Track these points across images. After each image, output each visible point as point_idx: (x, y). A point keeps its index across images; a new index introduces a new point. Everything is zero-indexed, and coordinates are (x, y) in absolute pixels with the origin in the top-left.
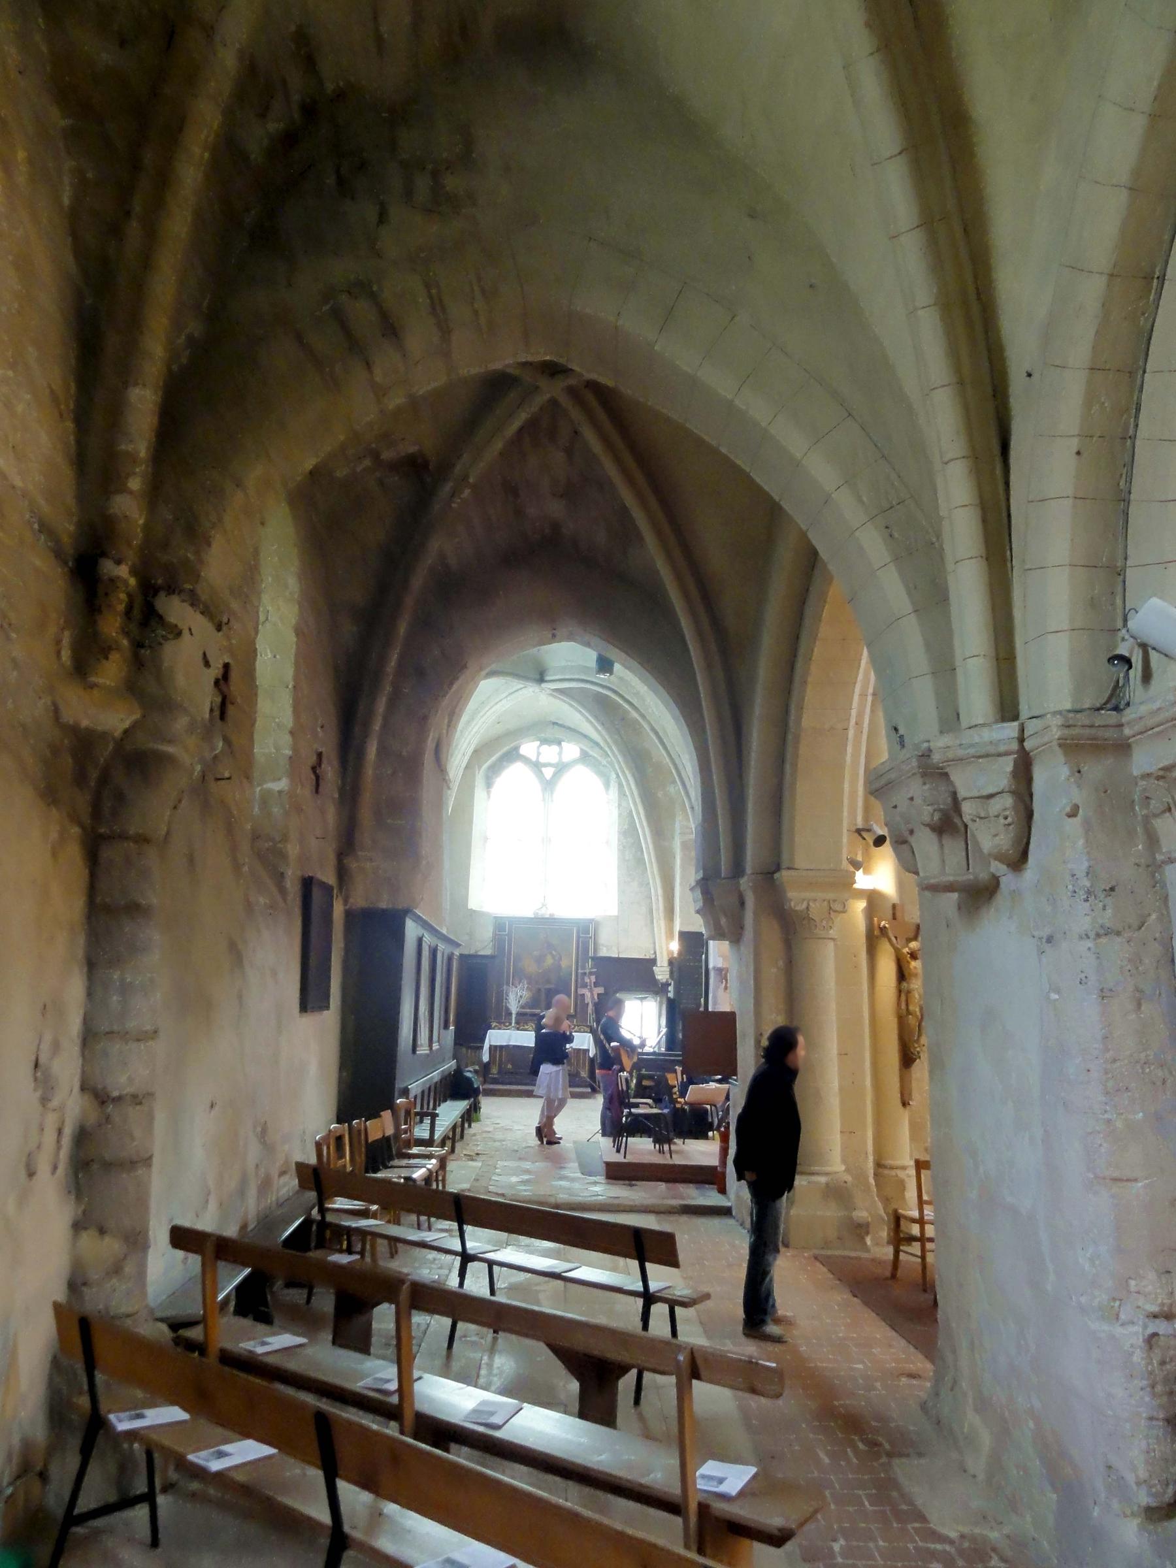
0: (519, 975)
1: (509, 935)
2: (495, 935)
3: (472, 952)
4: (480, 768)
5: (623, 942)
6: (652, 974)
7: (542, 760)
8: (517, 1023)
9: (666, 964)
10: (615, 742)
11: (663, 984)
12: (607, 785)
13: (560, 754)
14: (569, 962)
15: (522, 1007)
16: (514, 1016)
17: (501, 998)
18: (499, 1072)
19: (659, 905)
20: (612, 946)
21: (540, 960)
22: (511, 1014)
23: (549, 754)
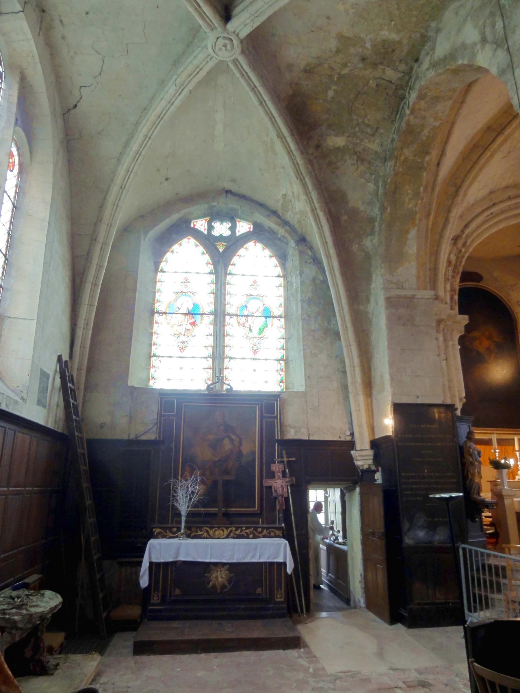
0: (190, 464)
2: (160, 415)
3: (132, 437)
4: (146, 233)
5: (314, 423)
6: (351, 458)
7: (216, 233)
8: (188, 528)
9: (368, 446)
11: (363, 471)
12: (282, 258)
13: (233, 229)
14: (251, 446)
15: (195, 506)
16: (183, 519)
17: (168, 494)
19: (354, 376)
21: (215, 445)
22: (179, 515)
23: (221, 229)
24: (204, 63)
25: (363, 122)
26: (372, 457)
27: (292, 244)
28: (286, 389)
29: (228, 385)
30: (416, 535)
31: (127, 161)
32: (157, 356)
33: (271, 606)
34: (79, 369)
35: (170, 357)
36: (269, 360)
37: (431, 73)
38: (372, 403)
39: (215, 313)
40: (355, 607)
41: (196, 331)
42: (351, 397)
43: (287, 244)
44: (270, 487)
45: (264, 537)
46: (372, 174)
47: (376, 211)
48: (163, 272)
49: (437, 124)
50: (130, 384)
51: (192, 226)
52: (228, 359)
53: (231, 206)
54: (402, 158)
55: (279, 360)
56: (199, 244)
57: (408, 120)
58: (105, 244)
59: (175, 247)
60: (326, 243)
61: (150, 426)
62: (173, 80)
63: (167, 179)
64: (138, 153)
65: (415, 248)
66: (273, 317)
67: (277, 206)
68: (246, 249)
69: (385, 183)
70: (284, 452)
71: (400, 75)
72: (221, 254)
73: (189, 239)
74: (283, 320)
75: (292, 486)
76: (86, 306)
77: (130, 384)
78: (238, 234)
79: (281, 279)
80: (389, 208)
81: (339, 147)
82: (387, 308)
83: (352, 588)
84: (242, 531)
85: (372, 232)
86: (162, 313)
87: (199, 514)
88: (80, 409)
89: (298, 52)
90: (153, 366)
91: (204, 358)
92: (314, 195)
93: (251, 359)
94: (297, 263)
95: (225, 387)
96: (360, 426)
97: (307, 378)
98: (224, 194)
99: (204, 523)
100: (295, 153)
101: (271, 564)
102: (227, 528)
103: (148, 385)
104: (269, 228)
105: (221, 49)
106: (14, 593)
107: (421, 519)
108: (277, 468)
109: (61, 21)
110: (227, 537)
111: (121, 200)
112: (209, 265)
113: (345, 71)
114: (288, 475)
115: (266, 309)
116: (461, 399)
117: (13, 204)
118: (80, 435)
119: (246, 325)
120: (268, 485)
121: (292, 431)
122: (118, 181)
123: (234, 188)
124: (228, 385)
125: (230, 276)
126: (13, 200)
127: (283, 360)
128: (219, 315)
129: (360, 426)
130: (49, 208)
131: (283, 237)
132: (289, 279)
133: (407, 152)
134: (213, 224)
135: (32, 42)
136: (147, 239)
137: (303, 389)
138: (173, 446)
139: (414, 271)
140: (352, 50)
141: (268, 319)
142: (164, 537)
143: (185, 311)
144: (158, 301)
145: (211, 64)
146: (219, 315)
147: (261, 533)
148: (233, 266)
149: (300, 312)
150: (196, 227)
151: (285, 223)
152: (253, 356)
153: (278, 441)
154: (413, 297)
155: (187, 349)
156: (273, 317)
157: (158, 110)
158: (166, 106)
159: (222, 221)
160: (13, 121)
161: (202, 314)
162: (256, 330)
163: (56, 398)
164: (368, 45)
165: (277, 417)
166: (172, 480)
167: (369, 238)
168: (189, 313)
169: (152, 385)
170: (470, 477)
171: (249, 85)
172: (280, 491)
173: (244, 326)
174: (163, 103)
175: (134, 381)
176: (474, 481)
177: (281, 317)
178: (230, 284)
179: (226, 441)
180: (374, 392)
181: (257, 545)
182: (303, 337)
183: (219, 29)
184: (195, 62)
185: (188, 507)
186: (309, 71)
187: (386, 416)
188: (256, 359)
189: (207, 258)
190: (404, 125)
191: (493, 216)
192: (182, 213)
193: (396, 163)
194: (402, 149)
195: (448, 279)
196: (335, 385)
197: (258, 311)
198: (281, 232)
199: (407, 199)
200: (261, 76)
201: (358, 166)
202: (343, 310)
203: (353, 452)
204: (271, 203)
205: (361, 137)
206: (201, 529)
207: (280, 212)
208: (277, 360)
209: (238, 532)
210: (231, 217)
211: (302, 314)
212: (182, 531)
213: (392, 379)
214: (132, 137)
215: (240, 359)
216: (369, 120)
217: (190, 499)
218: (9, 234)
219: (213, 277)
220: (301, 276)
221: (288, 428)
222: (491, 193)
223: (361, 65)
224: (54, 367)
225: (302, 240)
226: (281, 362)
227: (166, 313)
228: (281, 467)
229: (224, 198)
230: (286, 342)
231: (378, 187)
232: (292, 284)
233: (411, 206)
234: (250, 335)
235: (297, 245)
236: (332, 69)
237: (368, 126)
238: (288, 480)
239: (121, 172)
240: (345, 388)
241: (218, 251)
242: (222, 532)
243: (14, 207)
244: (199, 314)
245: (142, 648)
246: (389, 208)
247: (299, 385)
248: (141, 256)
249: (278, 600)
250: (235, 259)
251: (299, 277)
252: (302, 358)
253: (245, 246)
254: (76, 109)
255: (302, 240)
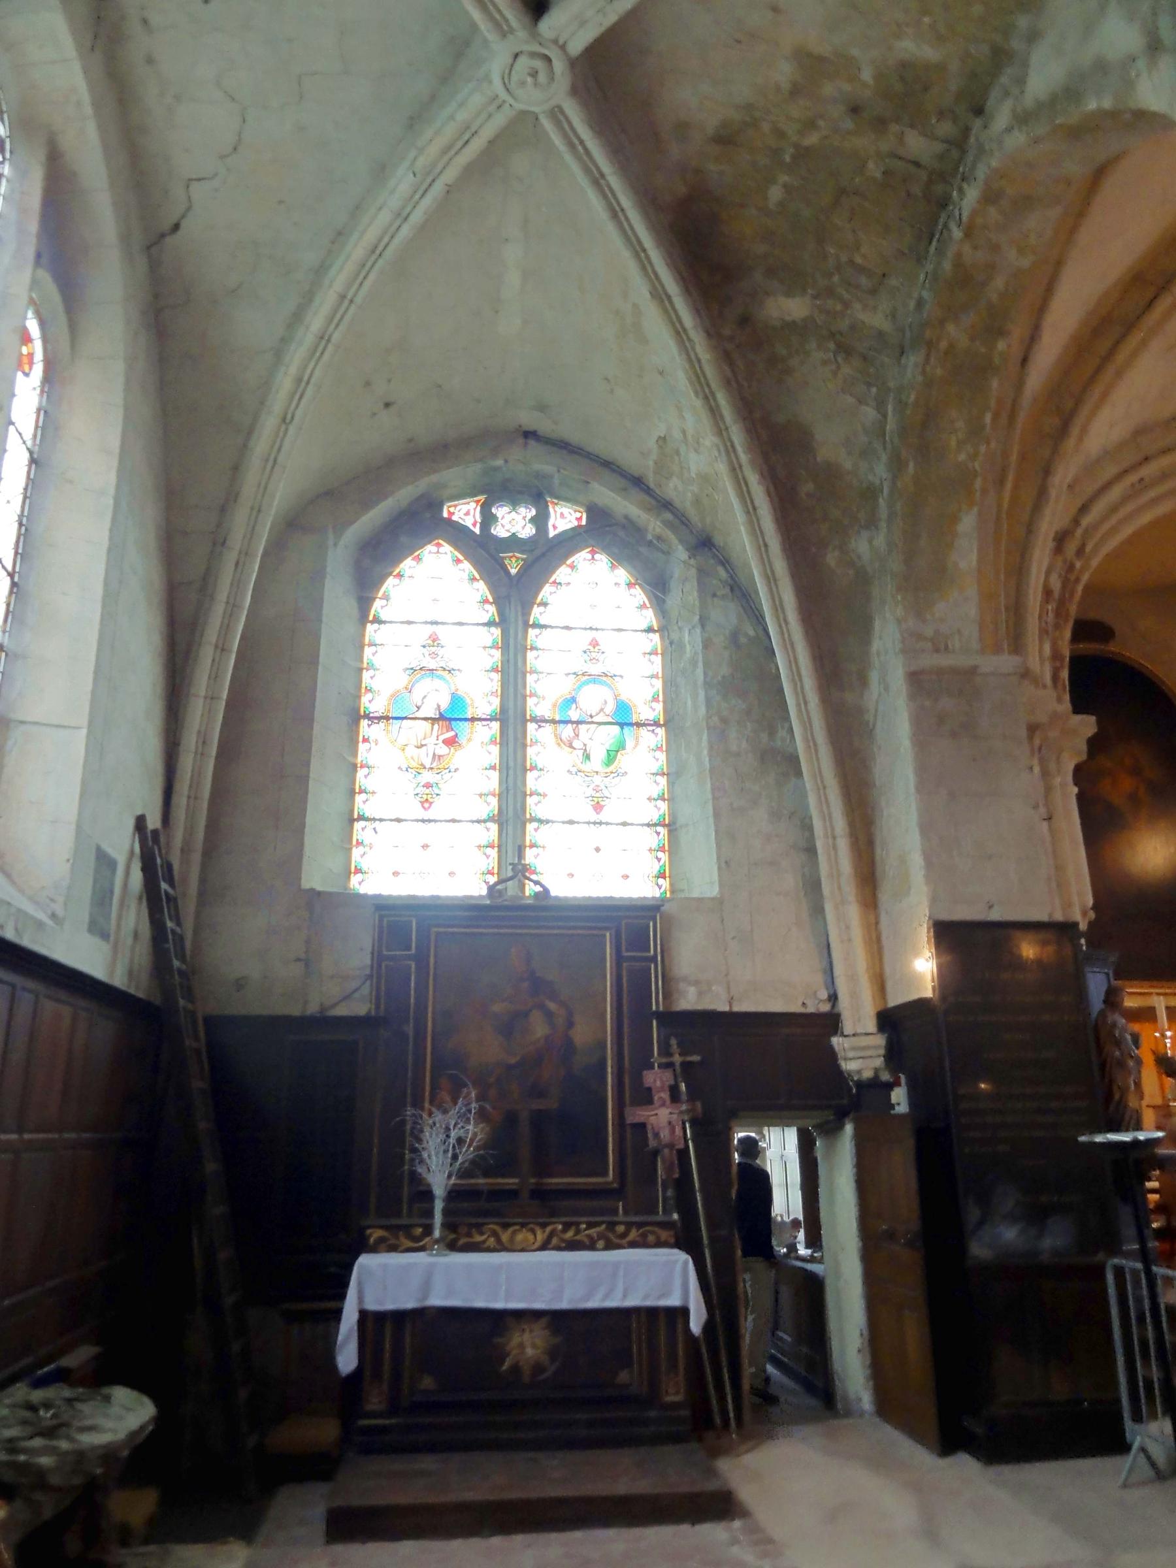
0: (450, 1076)
1: (421, 960)
2: (378, 958)
3: (312, 1009)
5: (742, 972)
6: (832, 1055)
7: (500, 531)
8: (448, 1226)
9: (871, 1025)
10: (727, 383)
11: (860, 1085)
12: (657, 587)
13: (540, 521)
14: (596, 1028)
15: (464, 1173)
16: (439, 1206)
17: (401, 1143)
18: (394, 1408)
20: (706, 979)
21: (510, 1027)
22: (428, 1195)
23: (514, 521)
24: (484, 116)
25: (851, 262)
26: (882, 1052)
27: (681, 553)
28: (672, 892)
29: (536, 883)
30: (999, 1237)
31: (296, 356)
32: (367, 819)
33: (653, 1414)
34: (186, 850)
35: (398, 820)
36: (632, 824)
37: (1018, 139)
38: (877, 923)
39: (502, 717)
40: (848, 1414)
41: (458, 758)
42: (829, 908)
43: (667, 553)
44: (643, 1126)
45: (633, 1245)
46: (869, 385)
47: (880, 472)
48: (381, 622)
49: (1025, 263)
50: (306, 884)
51: (445, 515)
52: (535, 825)
53: (537, 466)
54: (944, 345)
55: (655, 825)
56: (461, 557)
57: (959, 255)
58: (246, 553)
59: (407, 565)
60: (766, 545)
61: (354, 985)
62: (406, 164)
63: (387, 405)
64: (323, 338)
65: (974, 557)
66: (638, 725)
67: (645, 466)
68: (572, 567)
69: (901, 405)
70: (673, 1042)
71: (939, 147)
72: (515, 581)
73: (438, 545)
74: (661, 731)
75: (694, 1123)
76: (201, 702)
77: (306, 884)
78: (552, 533)
79: (656, 637)
80: (911, 465)
81: (794, 322)
82: (912, 697)
83: (837, 1365)
84: (578, 1232)
85: (872, 523)
86: (380, 718)
87: (472, 1194)
88: (188, 944)
89: (701, 93)
90: (359, 843)
91: (478, 822)
92: (737, 435)
93: (589, 823)
94: (693, 597)
95: (530, 889)
96: (852, 978)
97: (723, 865)
98: (521, 441)
99: (487, 1214)
100: (693, 334)
101: (652, 1313)
102: (544, 1226)
103: (346, 887)
104: (626, 517)
105: (523, 83)
106: (37, 1395)
107: (1008, 1199)
108: (656, 1079)
109: (145, 22)
110: (544, 1247)
111: (284, 449)
112: (487, 607)
113: (812, 139)
114: (684, 1097)
115: (623, 707)
116: (1084, 914)
117: (31, 452)
118: (190, 1006)
119: (576, 744)
120: (636, 1120)
121: (692, 991)
122: (278, 401)
123: (544, 426)
124: (536, 883)
125: (537, 631)
126: (29, 443)
127: (664, 825)
128: (511, 721)
129: (852, 978)
130: (115, 463)
131: (659, 538)
132: (675, 636)
133: (956, 333)
134: (494, 510)
135: (77, 67)
136: (342, 543)
137: (715, 891)
138: (410, 1029)
139: (972, 610)
140: (828, 89)
141: (626, 729)
142: (393, 1248)
143: (432, 713)
144: (368, 690)
145: (500, 120)
146: (512, 720)
147: (624, 1235)
148: (542, 609)
149: (702, 711)
150: (455, 518)
151: (666, 505)
152: (594, 817)
153: (659, 1016)
154: (973, 671)
155: (438, 803)
156: (638, 725)
157: (371, 235)
158: (391, 225)
159: (515, 504)
160: (30, 251)
161: (473, 720)
162: (598, 755)
163: (133, 918)
164: (867, 75)
165: (654, 959)
166: (410, 1111)
167: (865, 534)
168: (442, 718)
169: (357, 886)
170: (1117, 1097)
171: (587, 170)
172: (665, 1135)
173: (571, 746)
174: (384, 217)
175: (314, 878)
176: (1126, 1106)
177: (656, 724)
178: (536, 649)
179: (537, 1018)
180: (884, 897)
181: (616, 1265)
182: (712, 770)
183: (522, 34)
184: (462, 116)
185: (449, 1177)
186: (726, 139)
187: (917, 954)
188: (601, 823)
189: (482, 588)
190: (947, 265)
191: (1143, 485)
192: (423, 485)
193: (928, 355)
194: (942, 322)
195: (1047, 632)
196: (790, 881)
197: (602, 710)
198: (654, 525)
199: (953, 443)
200: (616, 151)
201: (839, 368)
202: (806, 703)
203: (835, 1041)
204: (630, 460)
205: (846, 296)
206: (479, 1227)
207: (651, 481)
208: (648, 825)
209: (570, 1234)
210: (537, 495)
211: (709, 717)
212: (437, 1233)
213: (929, 864)
214: (311, 300)
215: (564, 822)
216: (864, 256)
217: (455, 1157)
218: (21, 525)
219: (497, 632)
220: (703, 626)
221: (682, 986)
222: (1140, 432)
223: (849, 124)
224: (127, 847)
225: (704, 544)
226: (659, 829)
227: (387, 718)
228: (668, 1077)
229: (519, 448)
230: (671, 784)
231: (885, 416)
232: (681, 646)
233: (962, 457)
234: (587, 767)
235: (692, 556)
236: (780, 134)
237: (861, 270)
238: (684, 1107)
239: (284, 383)
240: (813, 887)
241: (507, 573)
242: (530, 1237)
243: (33, 461)
244: (466, 720)
245: (348, 1526)
246: (911, 465)
247: (705, 881)
248: (328, 583)
249: (670, 1399)
250: (546, 591)
251: (698, 630)
252: (711, 820)
253: (568, 562)
254: (179, 233)
255: (704, 544)
